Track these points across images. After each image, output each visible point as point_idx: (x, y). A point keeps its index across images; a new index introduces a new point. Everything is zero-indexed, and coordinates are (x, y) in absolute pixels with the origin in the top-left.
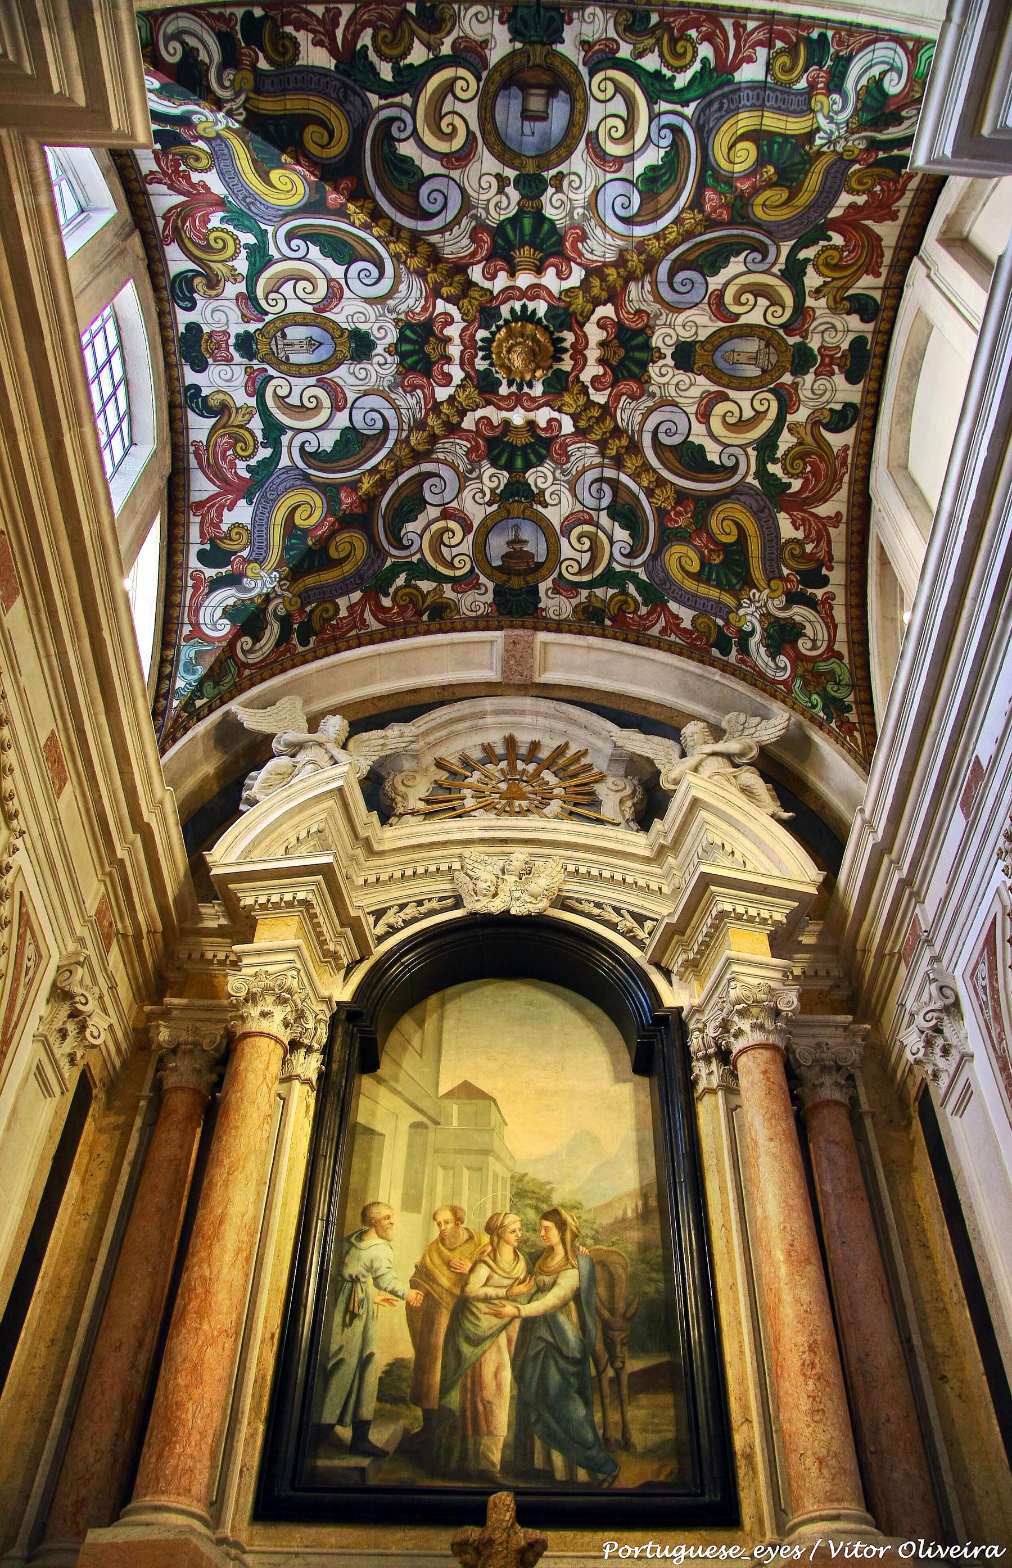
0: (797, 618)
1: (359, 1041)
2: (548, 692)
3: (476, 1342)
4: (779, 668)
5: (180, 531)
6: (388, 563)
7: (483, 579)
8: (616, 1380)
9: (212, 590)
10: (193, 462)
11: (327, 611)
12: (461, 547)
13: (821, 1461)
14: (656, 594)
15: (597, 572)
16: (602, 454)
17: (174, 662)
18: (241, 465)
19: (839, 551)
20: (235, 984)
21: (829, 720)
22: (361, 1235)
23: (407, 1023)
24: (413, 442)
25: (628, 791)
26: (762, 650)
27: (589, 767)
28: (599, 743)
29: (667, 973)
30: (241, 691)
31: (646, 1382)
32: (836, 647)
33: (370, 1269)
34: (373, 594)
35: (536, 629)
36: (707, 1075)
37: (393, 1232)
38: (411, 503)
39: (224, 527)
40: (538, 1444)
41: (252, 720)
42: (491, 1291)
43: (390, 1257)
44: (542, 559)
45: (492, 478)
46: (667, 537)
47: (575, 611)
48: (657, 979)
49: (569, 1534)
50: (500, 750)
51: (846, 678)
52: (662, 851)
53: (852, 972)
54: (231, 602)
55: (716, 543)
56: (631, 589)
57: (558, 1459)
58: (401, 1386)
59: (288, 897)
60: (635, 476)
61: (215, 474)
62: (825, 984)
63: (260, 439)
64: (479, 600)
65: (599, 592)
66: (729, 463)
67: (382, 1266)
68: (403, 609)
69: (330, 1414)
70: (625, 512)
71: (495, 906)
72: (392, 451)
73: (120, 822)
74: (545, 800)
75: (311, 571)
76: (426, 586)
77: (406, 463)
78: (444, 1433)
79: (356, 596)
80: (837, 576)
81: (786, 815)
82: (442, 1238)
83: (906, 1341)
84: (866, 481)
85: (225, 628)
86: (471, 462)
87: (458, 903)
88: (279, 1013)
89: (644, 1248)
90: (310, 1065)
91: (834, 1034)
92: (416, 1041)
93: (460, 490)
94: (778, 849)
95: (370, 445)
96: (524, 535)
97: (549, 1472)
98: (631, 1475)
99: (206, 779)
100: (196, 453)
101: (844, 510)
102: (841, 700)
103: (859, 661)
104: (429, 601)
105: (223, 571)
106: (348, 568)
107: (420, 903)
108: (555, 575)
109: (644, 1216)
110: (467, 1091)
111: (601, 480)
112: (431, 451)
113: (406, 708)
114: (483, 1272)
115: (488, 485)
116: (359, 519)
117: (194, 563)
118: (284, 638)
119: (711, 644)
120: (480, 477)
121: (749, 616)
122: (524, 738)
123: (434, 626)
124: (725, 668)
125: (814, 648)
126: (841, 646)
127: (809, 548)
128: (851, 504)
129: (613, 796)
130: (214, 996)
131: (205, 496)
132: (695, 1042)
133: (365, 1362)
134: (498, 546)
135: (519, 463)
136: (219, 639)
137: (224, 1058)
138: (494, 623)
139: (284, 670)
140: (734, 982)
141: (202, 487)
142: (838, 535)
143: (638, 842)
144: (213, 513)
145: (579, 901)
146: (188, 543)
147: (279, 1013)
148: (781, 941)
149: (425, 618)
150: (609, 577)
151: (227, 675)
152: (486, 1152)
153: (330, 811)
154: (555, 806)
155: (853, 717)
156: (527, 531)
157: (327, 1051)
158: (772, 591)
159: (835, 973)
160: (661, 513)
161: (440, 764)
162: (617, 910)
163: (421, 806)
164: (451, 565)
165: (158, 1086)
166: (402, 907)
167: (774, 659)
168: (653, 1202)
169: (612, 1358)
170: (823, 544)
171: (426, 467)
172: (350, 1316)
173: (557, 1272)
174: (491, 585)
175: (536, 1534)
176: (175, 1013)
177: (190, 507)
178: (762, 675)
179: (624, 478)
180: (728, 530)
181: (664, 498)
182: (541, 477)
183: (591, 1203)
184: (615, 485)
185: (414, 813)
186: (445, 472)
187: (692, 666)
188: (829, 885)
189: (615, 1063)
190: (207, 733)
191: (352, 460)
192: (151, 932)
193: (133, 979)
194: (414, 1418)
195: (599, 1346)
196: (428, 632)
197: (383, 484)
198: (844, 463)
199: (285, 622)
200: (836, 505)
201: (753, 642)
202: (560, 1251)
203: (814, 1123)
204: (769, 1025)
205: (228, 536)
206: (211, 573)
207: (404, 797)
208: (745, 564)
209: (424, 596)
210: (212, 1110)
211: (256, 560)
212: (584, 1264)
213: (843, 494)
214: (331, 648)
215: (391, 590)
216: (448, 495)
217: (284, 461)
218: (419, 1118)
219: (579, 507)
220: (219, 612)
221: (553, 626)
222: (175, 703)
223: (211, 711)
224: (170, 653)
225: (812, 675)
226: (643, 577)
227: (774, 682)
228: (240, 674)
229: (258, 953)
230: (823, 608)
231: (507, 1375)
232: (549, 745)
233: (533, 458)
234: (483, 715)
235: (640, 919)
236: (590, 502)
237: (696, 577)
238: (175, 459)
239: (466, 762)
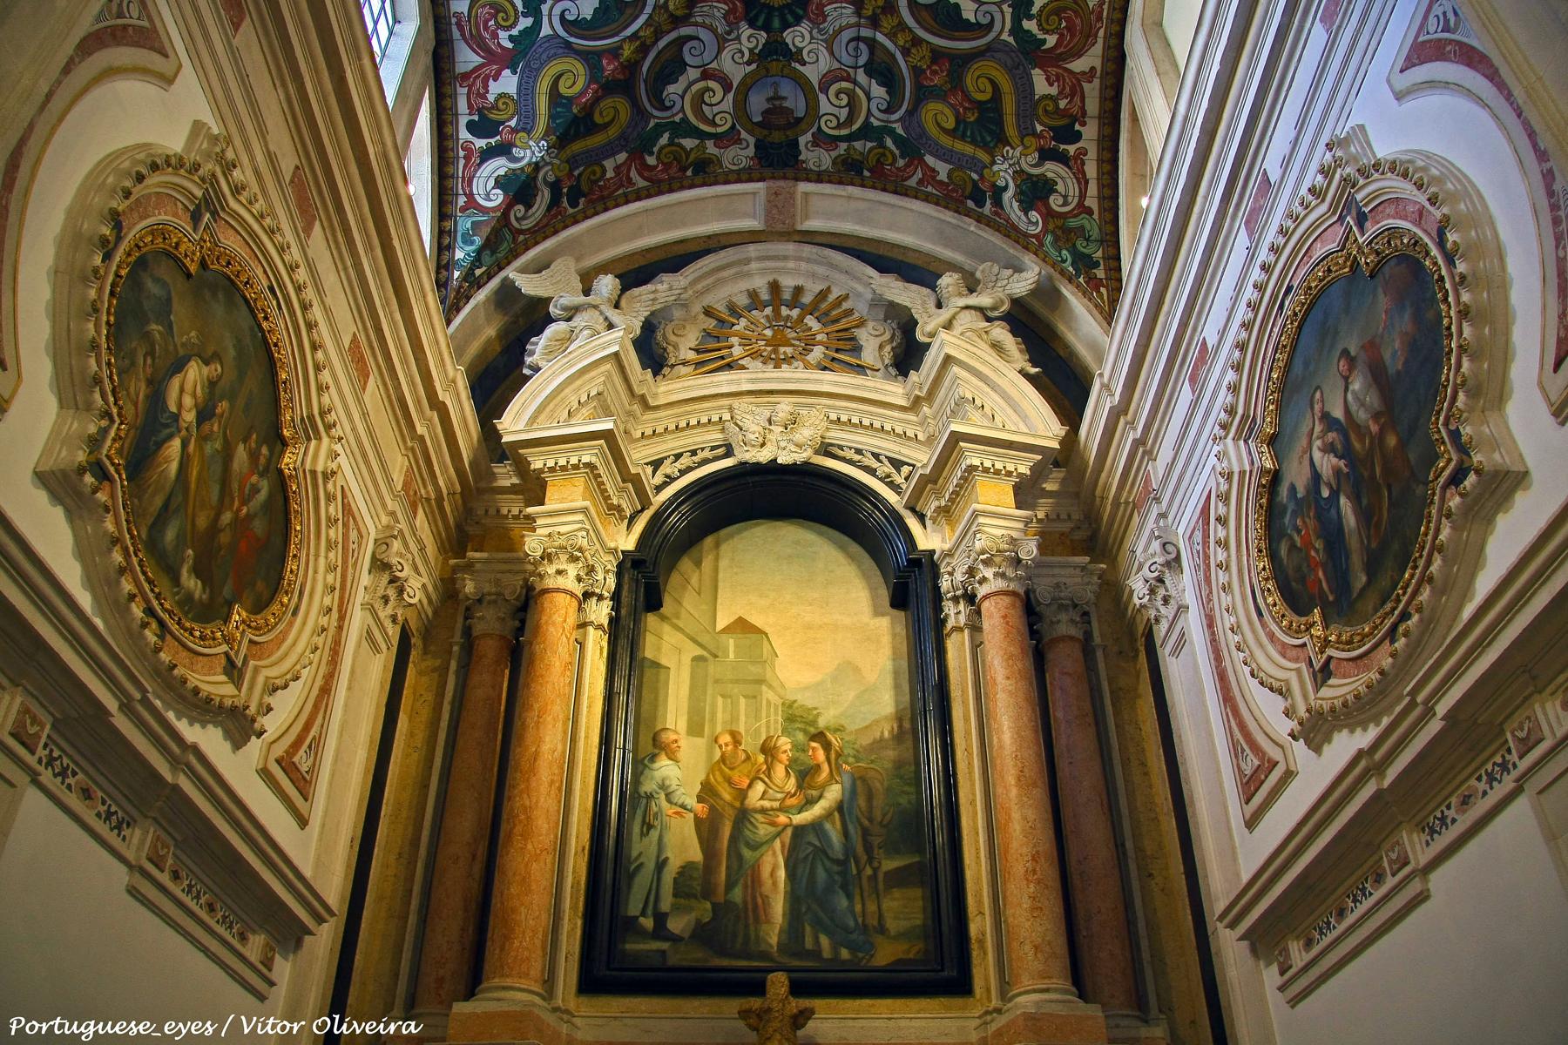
0: (1050, 175)
1: (644, 583)
2: (809, 238)
3: (755, 847)
4: (1032, 222)
5: (448, 103)
6: (652, 123)
7: (744, 135)
8: (874, 877)
9: (483, 161)
10: (456, 33)
11: (594, 173)
12: (721, 105)
13: (1036, 947)
14: (912, 148)
15: (855, 127)
16: (858, 13)
17: (452, 233)
18: (503, 35)
19: (1092, 106)
20: (533, 545)
21: (1078, 276)
22: (653, 758)
23: (686, 564)
24: (671, 7)
25: (887, 336)
26: (1016, 205)
27: (850, 312)
28: (860, 288)
29: (921, 518)
30: (516, 257)
31: (898, 879)
32: (1087, 203)
33: (663, 786)
34: (637, 155)
35: (797, 179)
36: (955, 614)
37: (681, 755)
38: (672, 67)
39: (491, 98)
40: (808, 929)
41: (529, 286)
42: (767, 804)
43: (679, 775)
44: (801, 114)
45: (750, 38)
46: (923, 94)
47: (834, 162)
49: (833, 1002)
50: (765, 296)
51: (1095, 234)
52: (915, 404)
53: (1091, 515)
54: (502, 172)
55: (971, 101)
56: (889, 142)
57: (825, 941)
58: (692, 884)
59: (574, 461)
60: (891, 36)
61: (478, 44)
62: (1065, 527)
63: (520, 8)
64: (741, 155)
65: (858, 145)
66: (984, 21)
67: (673, 784)
68: (667, 167)
69: (634, 908)
70: (882, 70)
71: (763, 456)
72: (651, 16)
73: (418, 402)
74: (809, 343)
75: (578, 136)
76: (688, 143)
77: (665, 28)
78: (728, 922)
79: (622, 157)
80: (1090, 131)
81: (1034, 370)
82: (723, 759)
83: (1119, 845)
84: (1121, 35)
85: (498, 198)
86: (729, 24)
87: (729, 453)
88: (572, 570)
89: (899, 765)
90: (601, 612)
92: (694, 580)
93: (719, 52)
94: (1025, 405)
95: (629, 11)
96: (783, 92)
97: (816, 954)
98: (885, 954)
99: (489, 342)
100: (459, 25)
101: (1098, 63)
102: (1089, 256)
103: (1108, 216)
104: (692, 157)
105: (492, 141)
106: (613, 132)
107: (694, 453)
108: (814, 129)
109: (899, 737)
110: (742, 626)
111: (858, 39)
112: (690, 15)
113: (675, 259)
114: (759, 787)
115: (746, 45)
116: (623, 85)
117: (464, 135)
118: (555, 201)
119: (969, 197)
120: (738, 38)
121: (1002, 172)
122: (788, 282)
123: (698, 180)
124: (980, 219)
125: (1065, 204)
126: (1092, 202)
127: (1062, 104)
128: (1105, 59)
129: (874, 343)
130: (511, 550)
131: (471, 67)
132: (945, 584)
133: (661, 865)
134: (757, 103)
135: (776, 23)
136: (493, 209)
137: (525, 605)
138: (756, 175)
139: (556, 232)
141: (467, 58)
142: (1092, 90)
143: (895, 392)
144: (479, 83)
145: (841, 448)
146: (457, 115)
147: (572, 570)
148: (1025, 492)
149: (689, 173)
150: (866, 131)
151: (503, 241)
152: (760, 681)
153: (609, 376)
154: (817, 353)
155: (1100, 273)
156: (787, 89)
157: (616, 597)
158: (1026, 148)
159: (1075, 516)
160: (917, 72)
161: (708, 312)
162: (876, 456)
163: (692, 355)
164: (713, 123)
165: (467, 632)
166: (678, 456)
167: (1026, 214)
168: (907, 725)
169: (870, 859)
170: (1077, 99)
171: (685, 31)
172: (648, 827)
173: (823, 788)
174: (752, 141)
175: (805, 1003)
176: (478, 566)
177: (456, 78)
178: (1015, 228)
179: (880, 37)
180: (982, 87)
181: (920, 57)
182: (799, 36)
183: (852, 727)
184: (872, 44)
185: (685, 363)
186: (703, 34)
187: (948, 216)
188: (1070, 440)
189: (874, 598)
190: (488, 299)
191: (614, 26)
192: (451, 494)
193: (437, 536)
194: (704, 910)
195: (860, 849)
196: (692, 187)
197: (644, 49)
198: (1100, 18)
199: (555, 187)
200: (1091, 60)
201: (1007, 196)
202: (826, 767)
203: (1050, 656)
204: (1010, 573)
205: (495, 107)
206: (481, 143)
207: (676, 347)
208: (1000, 123)
209: (688, 153)
210: (519, 650)
211: (524, 130)
212: (846, 779)
213: (1098, 49)
214: (600, 207)
215: (655, 149)
216: (707, 57)
217: (546, 30)
218: (699, 652)
219: (836, 65)
220: (491, 183)
221: (814, 177)
222: (456, 274)
223: (489, 279)
224: (448, 225)
225: (1063, 230)
226: (900, 131)
227: (1026, 235)
228: (515, 240)
229: (550, 514)
230: (1074, 164)
231: (782, 874)
232: (812, 289)
233: (790, 19)
234: (748, 261)
235: (897, 464)
236: (846, 59)
237: (951, 133)
238: (437, 31)
239: (733, 310)
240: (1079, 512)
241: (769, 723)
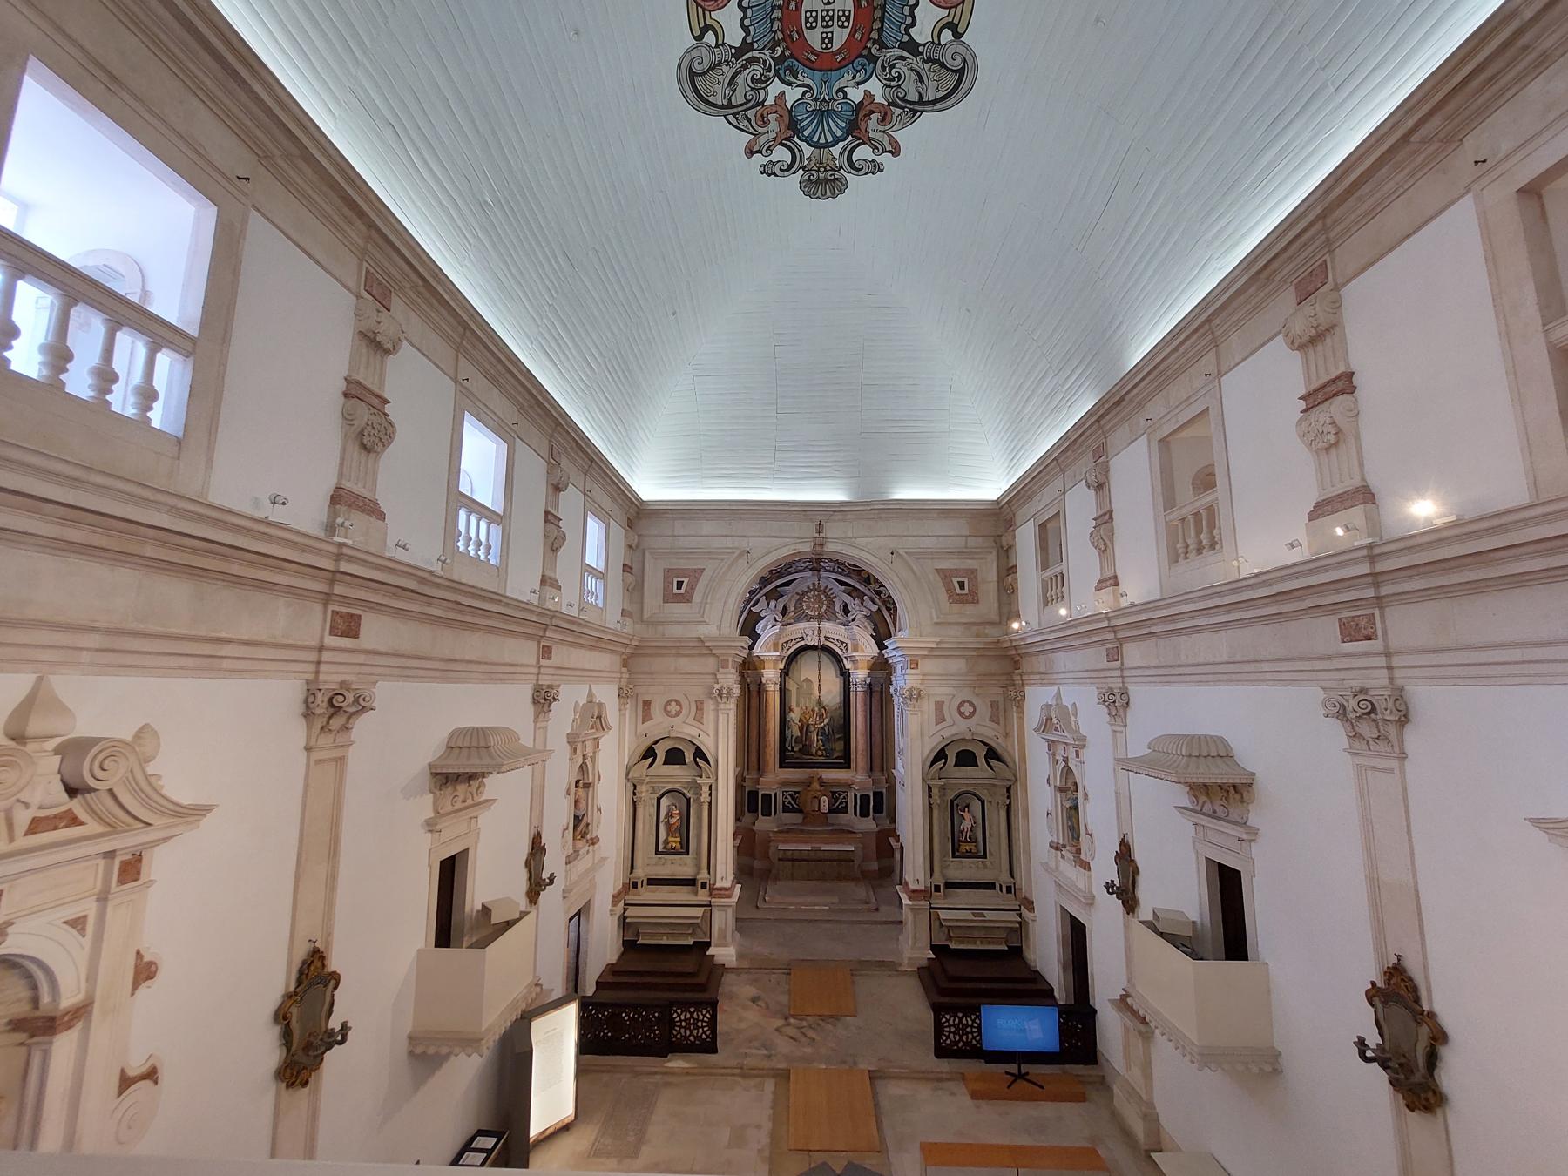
1: (785, 673)
43: (794, 716)
78: (806, 749)
91: (880, 674)
110: (807, 680)
113: (788, 584)
137: (760, 684)
140: (860, 675)
240: (882, 667)
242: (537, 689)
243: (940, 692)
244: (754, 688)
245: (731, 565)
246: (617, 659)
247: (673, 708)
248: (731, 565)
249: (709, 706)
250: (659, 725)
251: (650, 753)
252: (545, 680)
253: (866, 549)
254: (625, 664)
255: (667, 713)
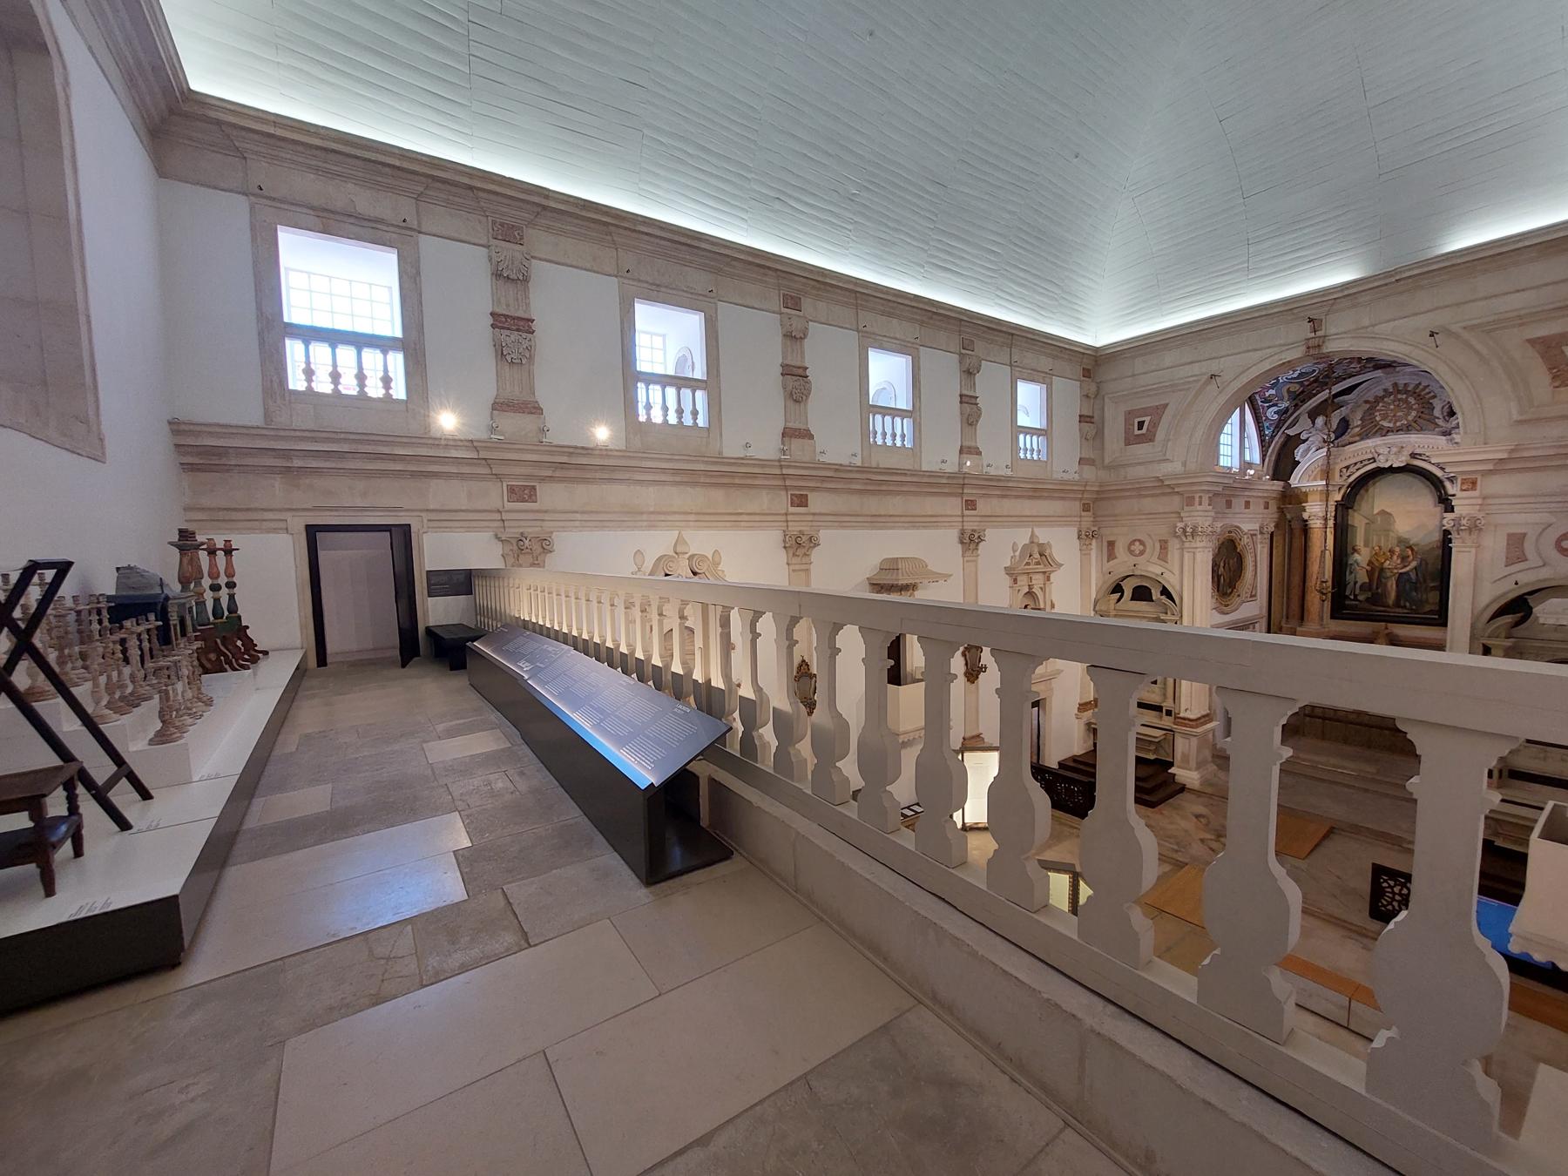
1: (1346, 506)
31: (1433, 588)
41: (1291, 432)
43: (1361, 558)
48: (1447, 484)
78: (1377, 598)
110: (1383, 512)
122: (1401, 382)
241: (1392, 543)
242: (962, 532)
243: (1523, 520)
244: (1296, 525)
245: (1196, 397)
246: (1077, 506)
247: (1137, 547)
248: (1196, 397)
249: (1174, 545)
250: (1123, 564)
251: (1118, 589)
252: (969, 527)
253: (1392, 335)
254: (1086, 508)
255: (1132, 552)
